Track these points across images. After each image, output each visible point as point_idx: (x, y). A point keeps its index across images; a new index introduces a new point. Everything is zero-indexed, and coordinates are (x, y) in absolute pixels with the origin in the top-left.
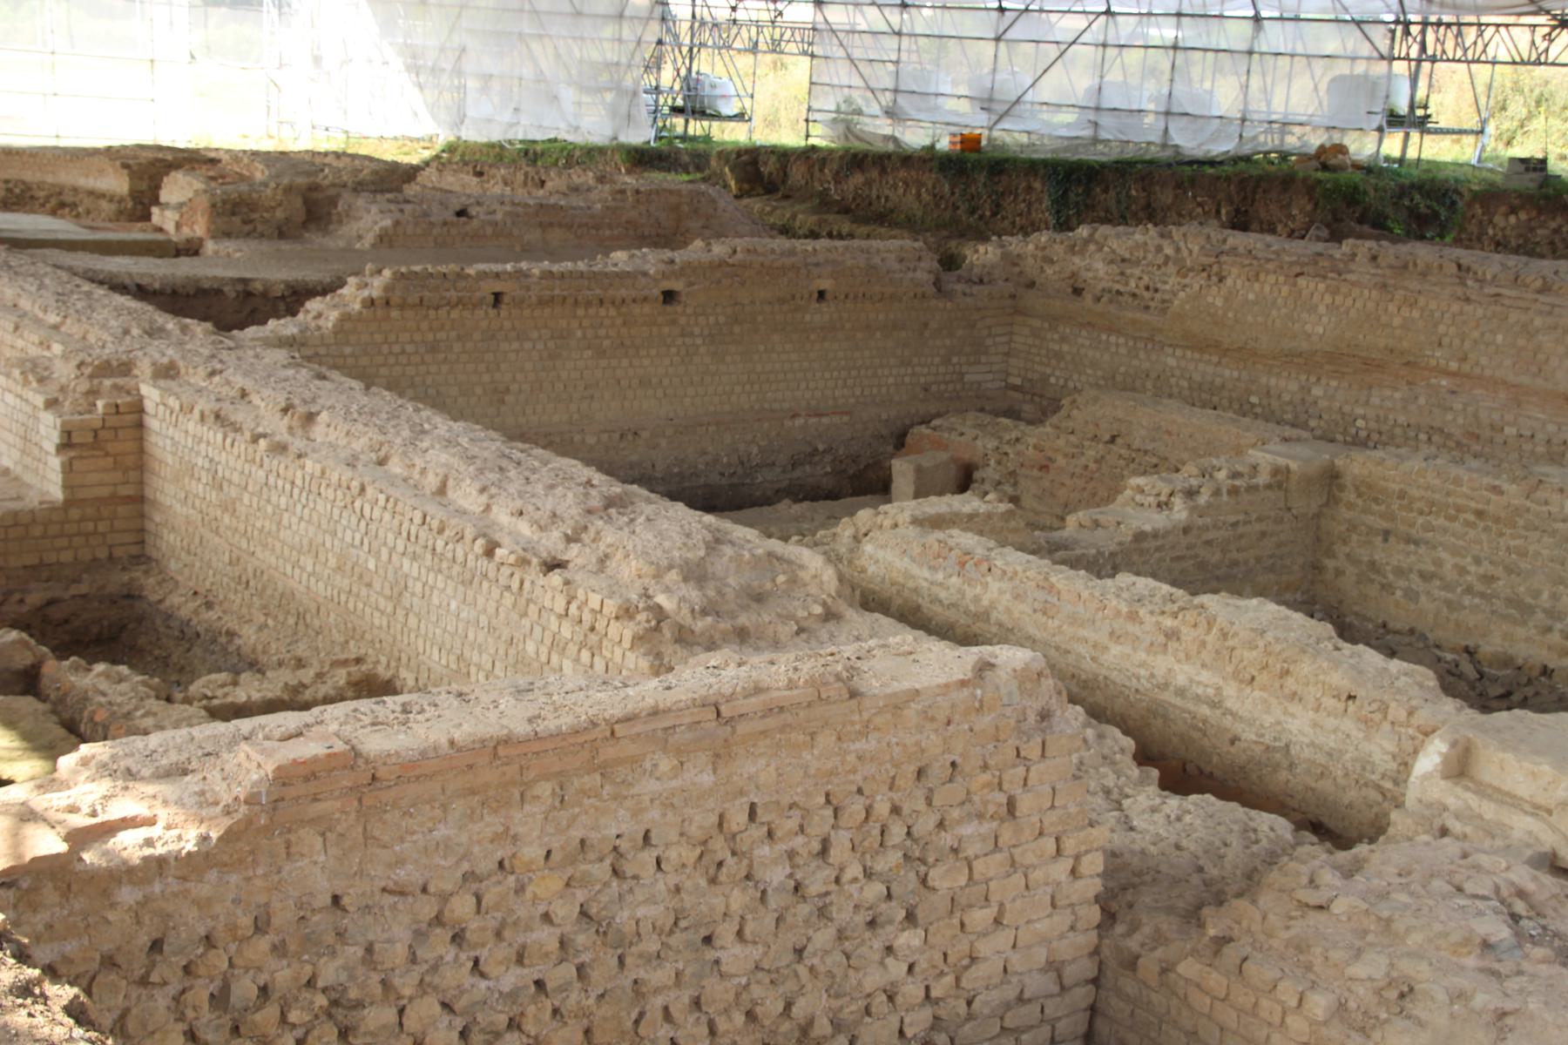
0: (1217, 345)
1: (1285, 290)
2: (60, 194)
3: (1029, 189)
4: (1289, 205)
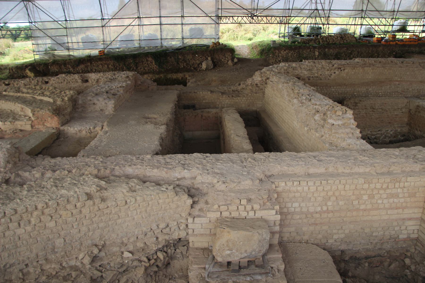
0: (345, 85)
1: (361, 70)
3: (147, 61)
4: (224, 55)
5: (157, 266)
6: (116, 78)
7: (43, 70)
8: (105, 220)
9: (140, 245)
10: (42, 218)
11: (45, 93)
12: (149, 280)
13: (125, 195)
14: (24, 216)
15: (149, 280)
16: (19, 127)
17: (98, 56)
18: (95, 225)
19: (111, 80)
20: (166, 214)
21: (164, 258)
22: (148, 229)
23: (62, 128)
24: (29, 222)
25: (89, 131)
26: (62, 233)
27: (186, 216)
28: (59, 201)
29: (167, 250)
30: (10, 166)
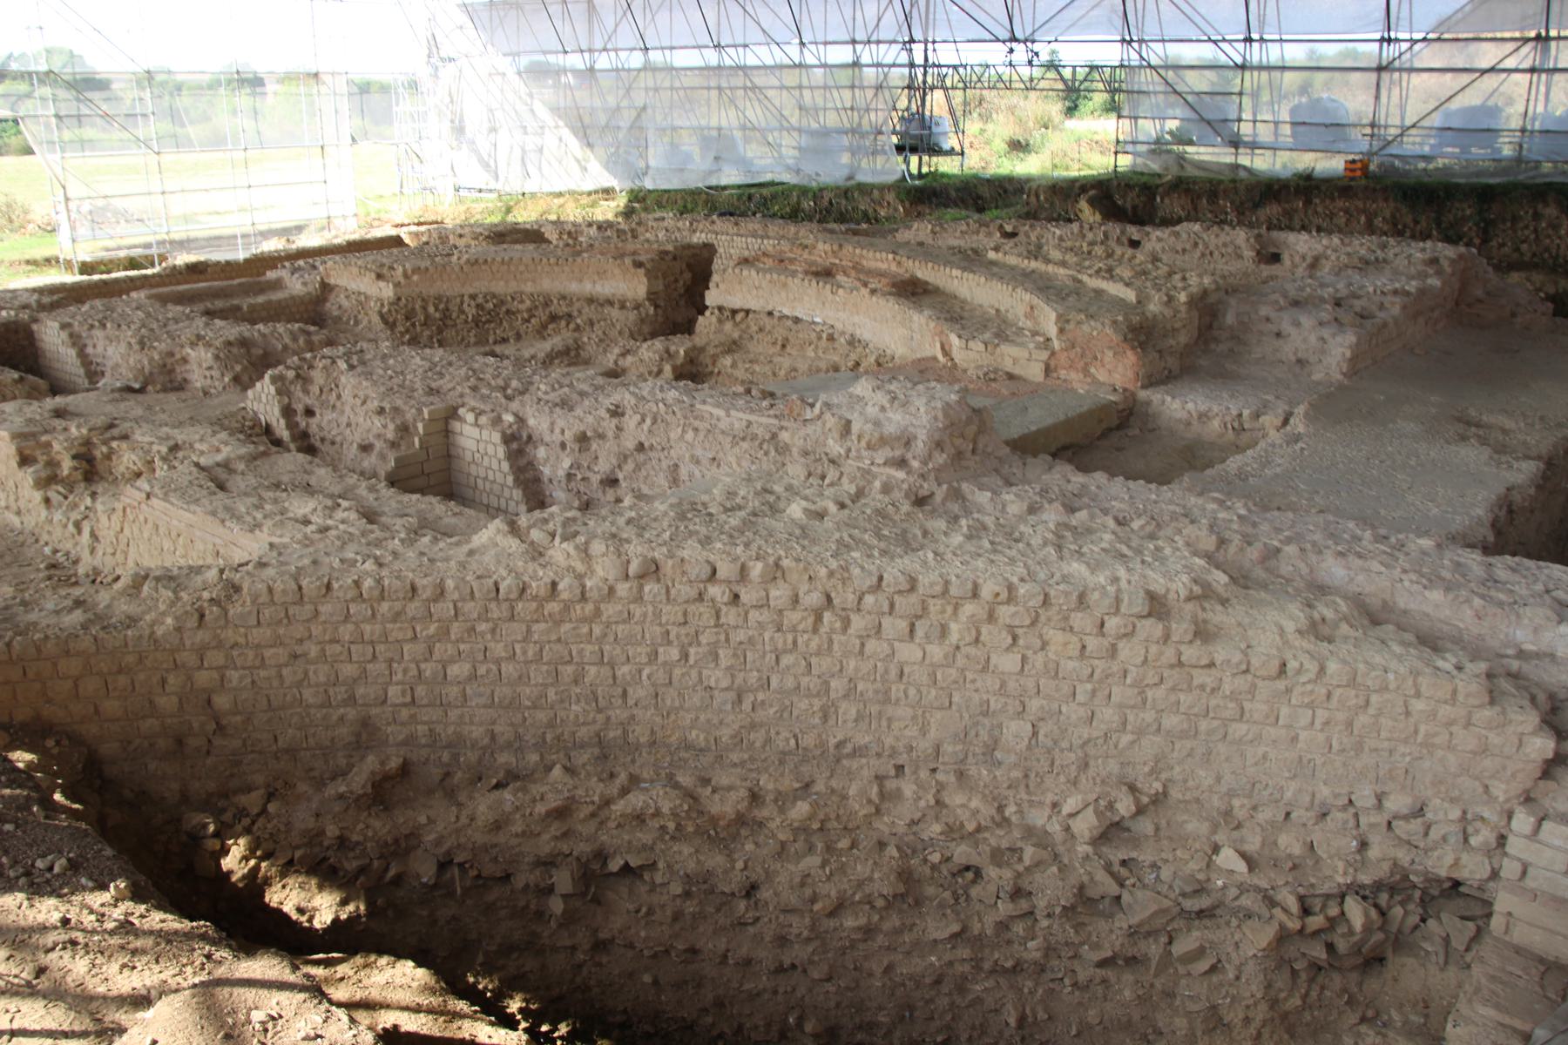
2: (547, 304)
5: (1330, 947)
6: (1385, 261)
7: (1134, 208)
8: (1190, 707)
9: (1289, 843)
10: (984, 630)
11: (1118, 271)
12: (1279, 984)
13: (1286, 642)
14: (934, 606)
15: (1279, 984)
16: (1008, 365)
17: (1339, 179)
18: (1149, 716)
19: (1367, 263)
20: (1427, 764)
21: (1367, 929)
22: (1336, 796)
23: (1143, 394)
24: (944, 631)
25: (1236, 425)
26: (1034, 705)
27: (1507, 800)
28: (1052, 593)
29: (1390, 908)
30: (940, 459)
